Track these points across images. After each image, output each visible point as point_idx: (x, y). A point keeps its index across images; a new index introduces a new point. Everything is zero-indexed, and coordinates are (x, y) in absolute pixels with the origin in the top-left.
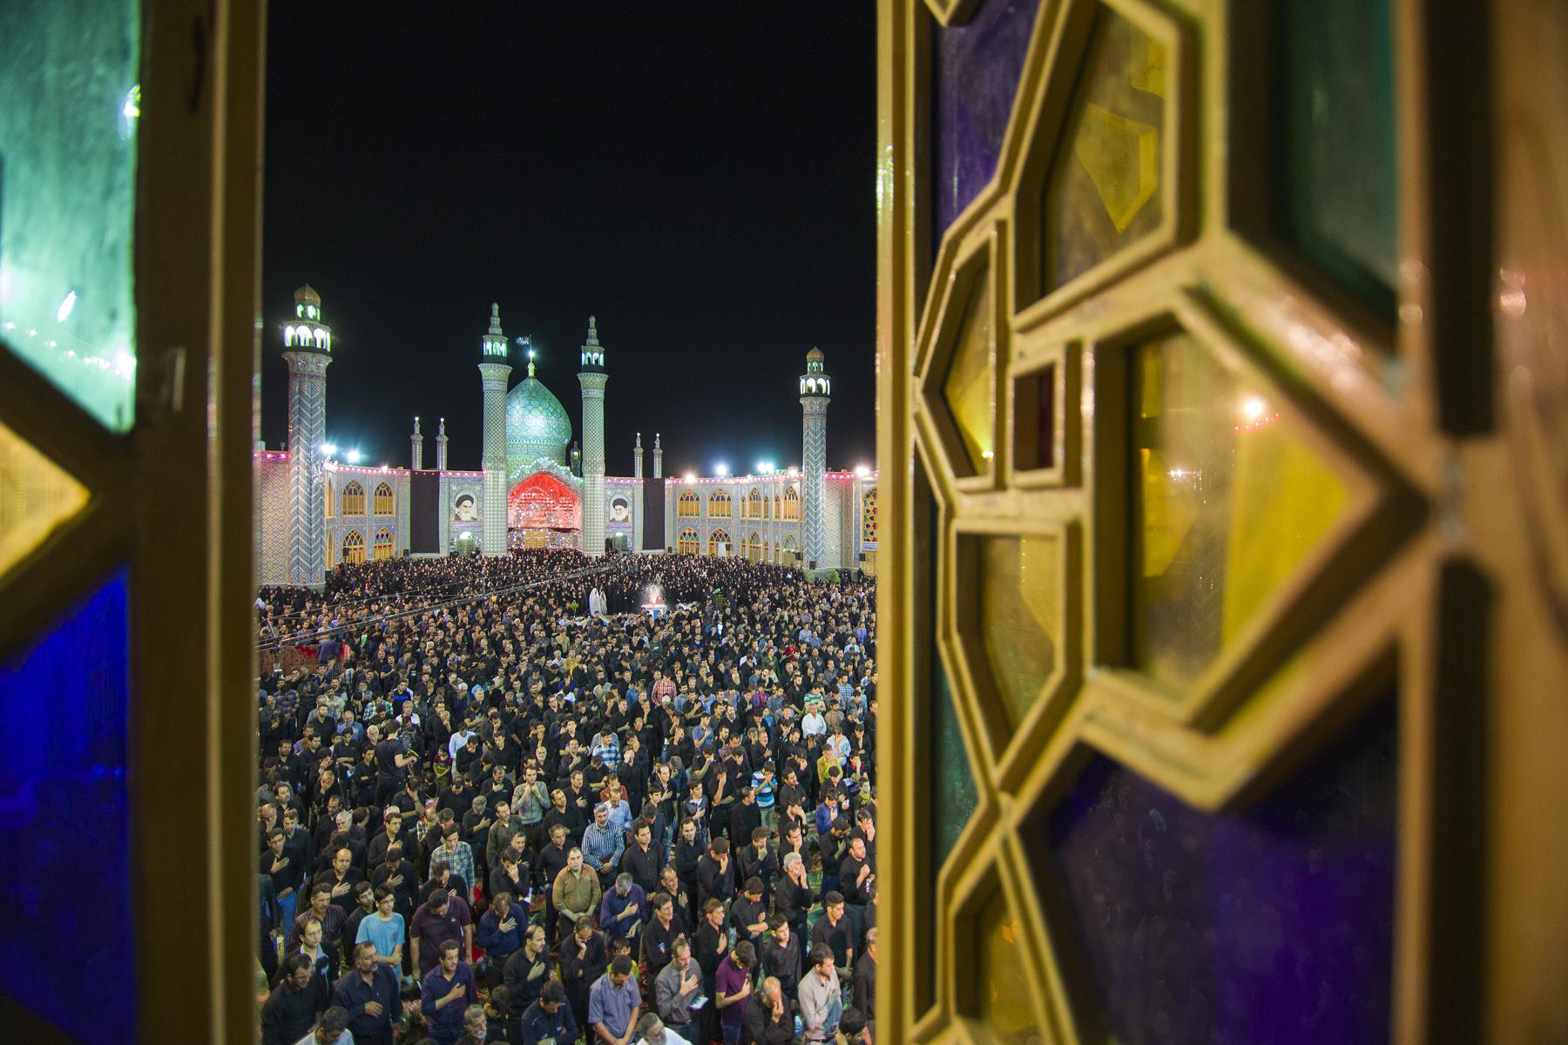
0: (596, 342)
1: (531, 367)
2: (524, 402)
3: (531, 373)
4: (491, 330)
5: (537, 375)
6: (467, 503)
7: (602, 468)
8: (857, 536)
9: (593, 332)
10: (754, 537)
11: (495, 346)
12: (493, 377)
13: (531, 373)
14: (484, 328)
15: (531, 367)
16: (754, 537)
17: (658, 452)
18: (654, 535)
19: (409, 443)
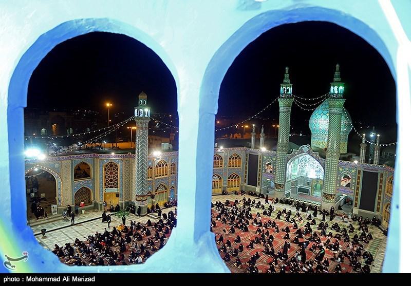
2: (320, 111)
4: (285, 81)
6: (270, 166)
9: (337, 74)
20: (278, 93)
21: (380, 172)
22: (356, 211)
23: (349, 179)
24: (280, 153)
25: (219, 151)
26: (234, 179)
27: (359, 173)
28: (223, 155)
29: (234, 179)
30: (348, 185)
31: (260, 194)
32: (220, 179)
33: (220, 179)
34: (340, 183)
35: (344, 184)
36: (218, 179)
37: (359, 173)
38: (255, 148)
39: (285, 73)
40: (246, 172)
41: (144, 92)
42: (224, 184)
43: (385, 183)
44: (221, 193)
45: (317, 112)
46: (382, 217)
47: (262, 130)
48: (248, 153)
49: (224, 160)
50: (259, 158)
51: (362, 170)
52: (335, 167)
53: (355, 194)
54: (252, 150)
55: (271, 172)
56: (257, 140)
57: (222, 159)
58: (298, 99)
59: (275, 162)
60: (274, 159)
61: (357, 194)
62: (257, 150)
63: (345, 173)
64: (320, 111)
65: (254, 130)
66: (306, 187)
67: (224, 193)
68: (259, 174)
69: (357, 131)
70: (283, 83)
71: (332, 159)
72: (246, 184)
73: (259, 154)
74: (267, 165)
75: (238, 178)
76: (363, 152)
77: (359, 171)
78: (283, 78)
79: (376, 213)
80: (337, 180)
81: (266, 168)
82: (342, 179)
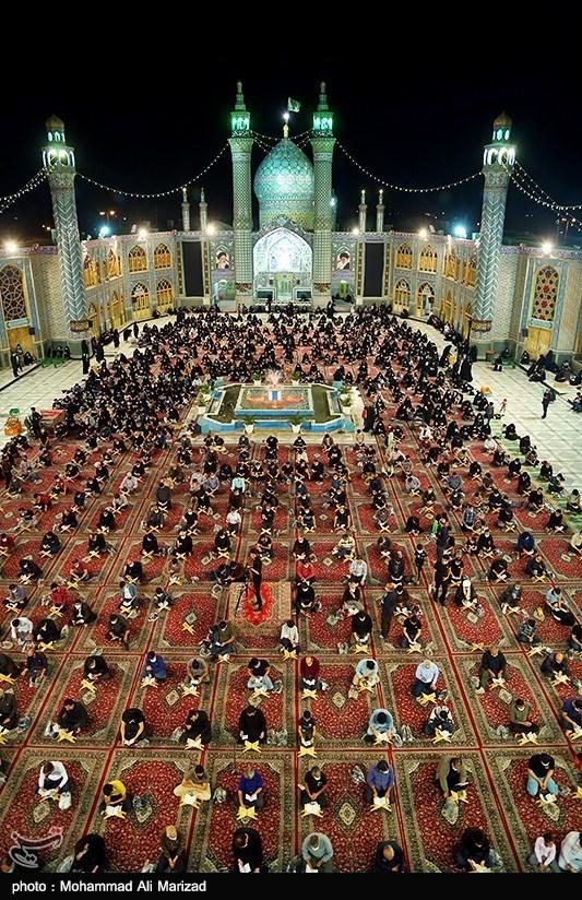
0: (323, 107)
1: (286, 129)
2: (277, 163)
3: (286, 135)
4: (238, 107)
5: (290, 135)
6: (223, 257)
7: (329, 225)
8: (526, 312)
10: (449, 298)
11: (240, 121)
12: (239, 151)
13: (286, 135)
14: (230, 107)
15: (286, 129)
16: (449, 298)
17: (380, 207)
18: (373, 285)
19: (181, 209)
20: (227, 132)
21: (385, 241)
22: (359, 300)
23: (347, 257)
24: (241, 232)
25: (139, 239)
26: (164, 290)
27: (361, 247)
28: (145, 247)
29: (164, 290)
30: (347, 267)
31: (211, 308)
32: (146, 291)
33: (146, 291)
34: (335, 267)
35: (341, 265)
36: (143, 293)
37: (361, 247)
38: (192, 229)
39: (237, 93)
40: (180, 275)
41: (57, 115)
42: (153, 300)
43: (393, 255)
44: (150, 316)
45: (269, 165)
46: (391, 302)
47: (203, 197)
48: (180, 240)
49: (147, 253)
50: (203, 246)
51: (364, 241)
52: (326, 244)
53: (352, 279)
54: (188, 234)
55: (227, 266)
56: (195, 215)
57: (144, 254)
58: (262, 139)
59: (232, 251)
60: (230, 244)
61: (360, 277)
62: (198, 232)
63: (341, 250)
64: (277, 163)
65: (185, 198)
66: (268, 288)
67: (156, 316)
68: (206, 275)
69: (382, 180)
70: (234, 110)
71: (325, 232)
72: (183, 297)
73: (202, 240)
74: (219, 257)
75: (170, 287)
76: (363, 216)
77: (361, 244)
78: (234, 102)
79: (384, 298)
80: (332, 262)
81: (218, 261)
82: (339, 259)
